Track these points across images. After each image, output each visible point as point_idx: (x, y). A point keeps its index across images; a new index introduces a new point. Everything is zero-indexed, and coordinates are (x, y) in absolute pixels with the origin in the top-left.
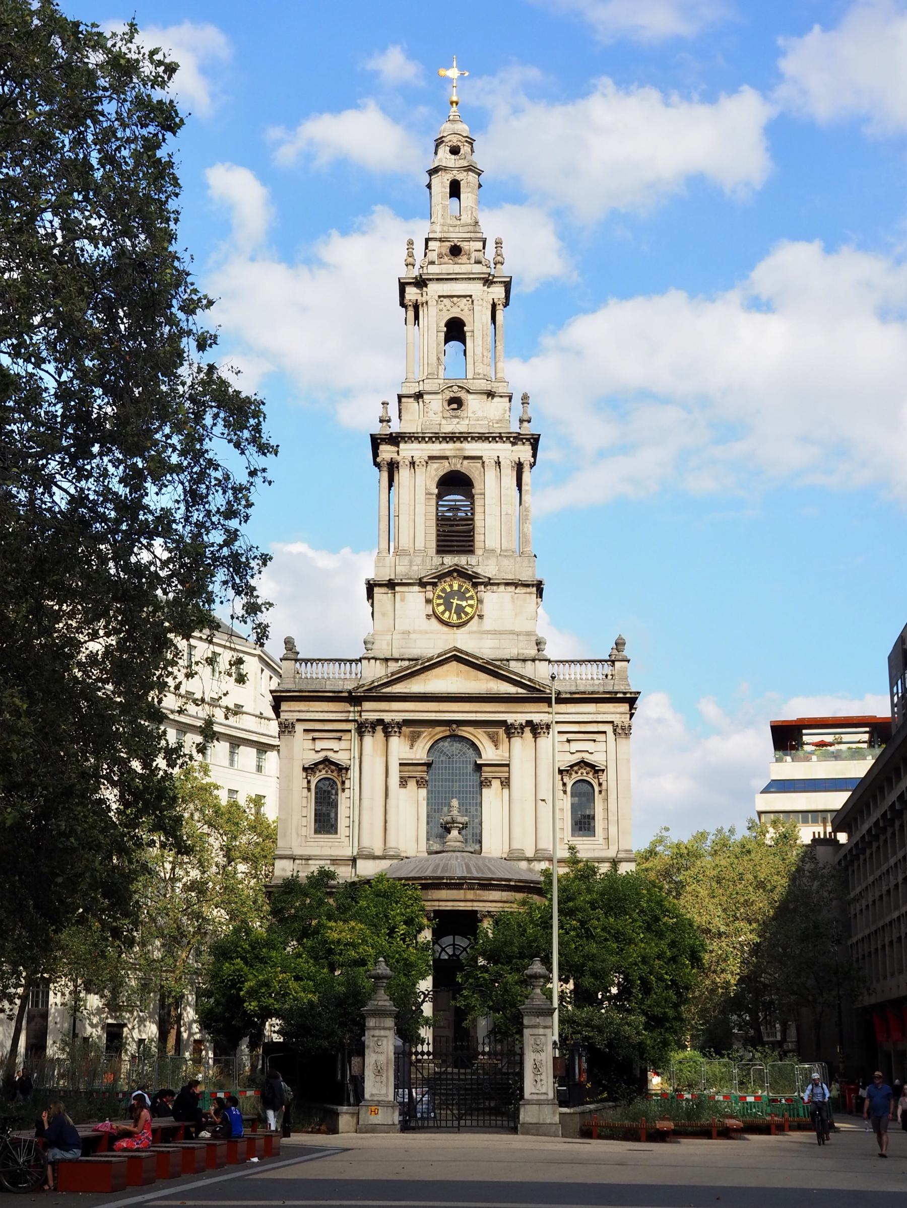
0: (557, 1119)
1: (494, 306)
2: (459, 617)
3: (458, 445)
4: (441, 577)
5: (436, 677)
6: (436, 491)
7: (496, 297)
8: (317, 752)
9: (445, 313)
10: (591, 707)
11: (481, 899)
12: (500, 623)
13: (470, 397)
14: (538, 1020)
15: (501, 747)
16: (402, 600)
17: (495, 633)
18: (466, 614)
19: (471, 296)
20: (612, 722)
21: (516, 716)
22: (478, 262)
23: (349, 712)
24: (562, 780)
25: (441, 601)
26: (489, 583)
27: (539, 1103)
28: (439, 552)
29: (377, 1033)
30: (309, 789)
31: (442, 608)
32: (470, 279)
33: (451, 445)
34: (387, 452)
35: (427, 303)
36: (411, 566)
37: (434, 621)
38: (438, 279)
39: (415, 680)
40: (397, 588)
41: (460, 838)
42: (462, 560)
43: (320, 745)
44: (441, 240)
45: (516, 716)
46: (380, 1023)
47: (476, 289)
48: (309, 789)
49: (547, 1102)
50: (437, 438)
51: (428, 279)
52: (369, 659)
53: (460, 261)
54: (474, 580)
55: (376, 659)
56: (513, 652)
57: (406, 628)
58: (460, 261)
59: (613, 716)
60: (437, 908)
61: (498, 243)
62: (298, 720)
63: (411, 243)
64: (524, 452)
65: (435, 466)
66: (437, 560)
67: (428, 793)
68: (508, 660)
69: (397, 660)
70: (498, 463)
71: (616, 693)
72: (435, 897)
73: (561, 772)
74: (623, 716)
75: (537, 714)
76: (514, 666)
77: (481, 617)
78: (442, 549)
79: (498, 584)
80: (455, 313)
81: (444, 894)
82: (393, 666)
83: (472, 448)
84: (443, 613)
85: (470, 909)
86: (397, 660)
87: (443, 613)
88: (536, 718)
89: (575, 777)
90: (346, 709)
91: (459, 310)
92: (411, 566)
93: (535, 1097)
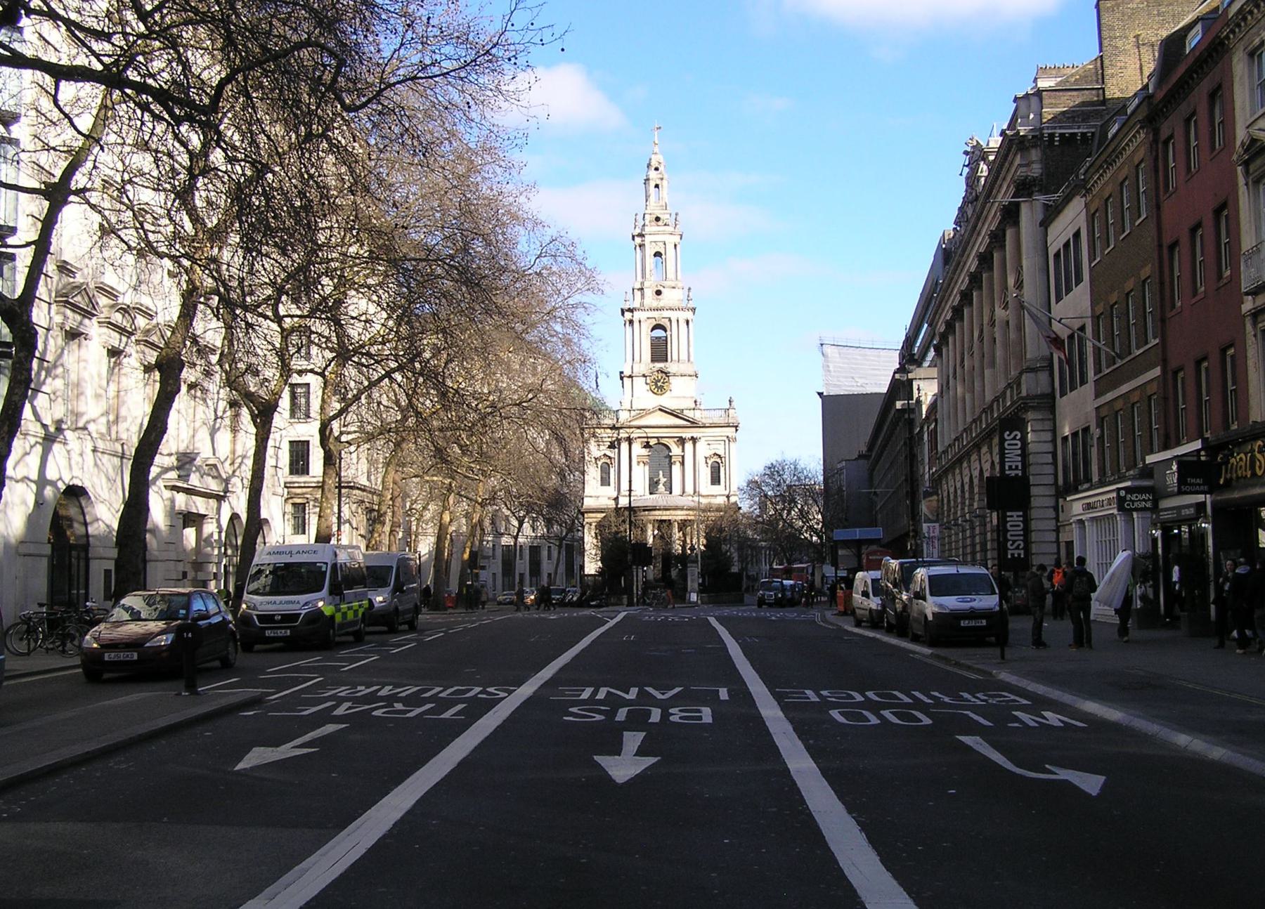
12: (679, 394)
28: (653, 361)
64: (689, 315)
66: (651, 365)
81: (657, 513)
82: (633, 413)
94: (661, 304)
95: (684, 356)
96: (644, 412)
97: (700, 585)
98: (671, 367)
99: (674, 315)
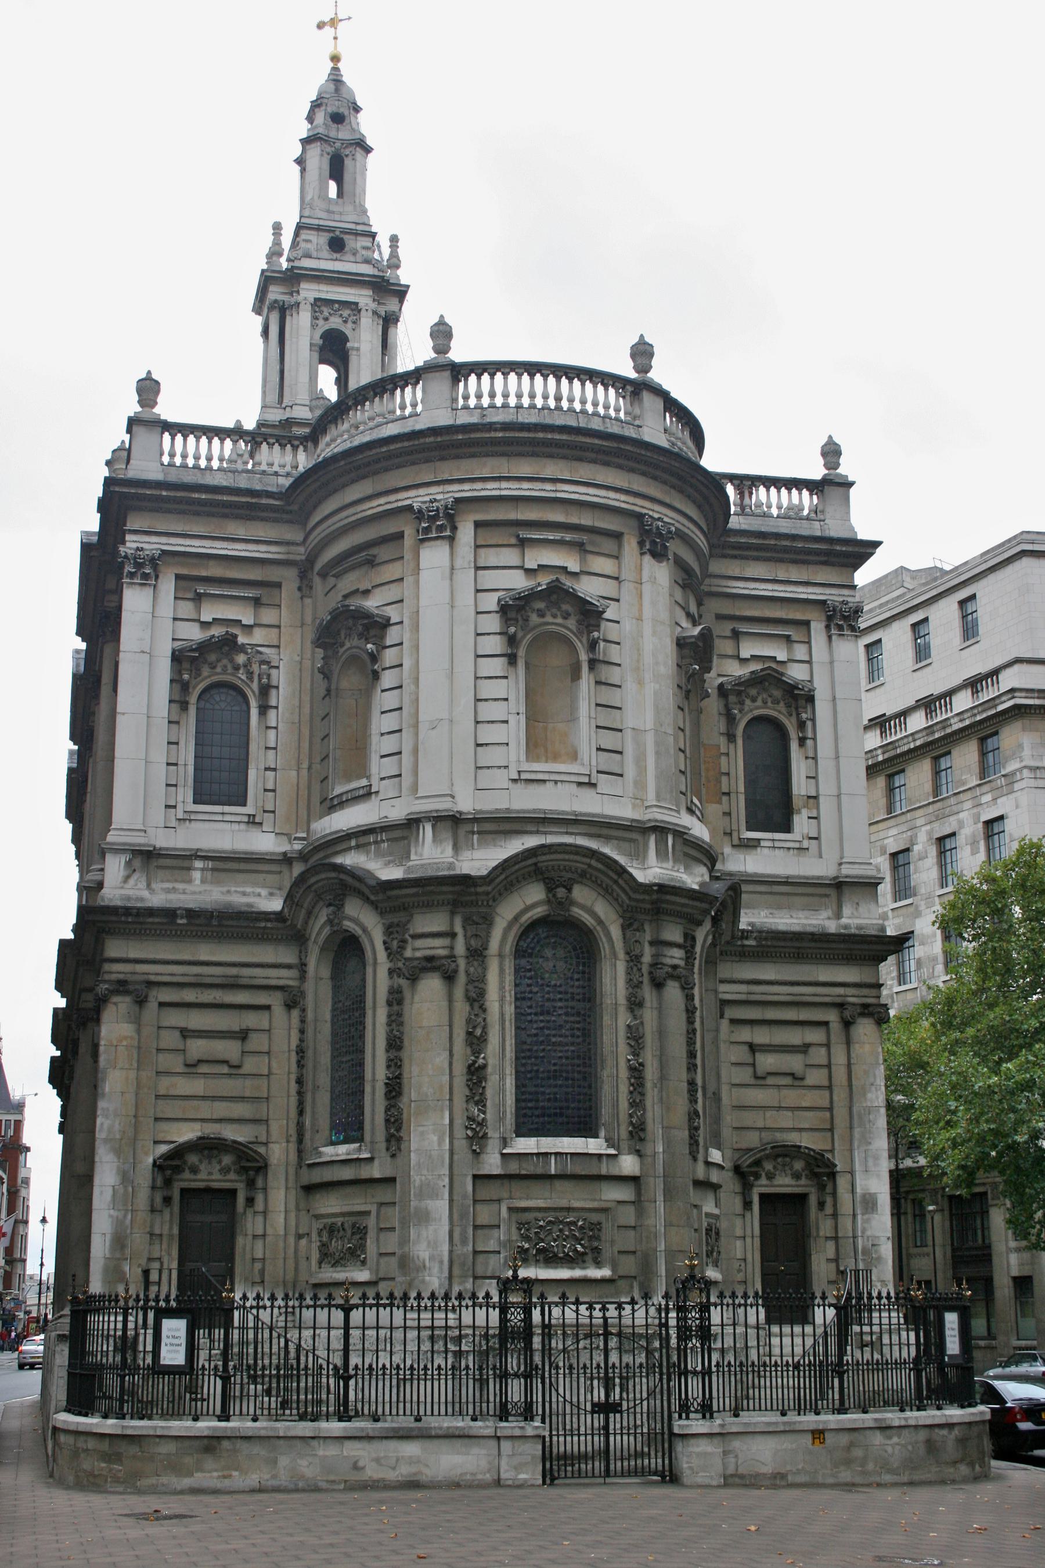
9: (321, 322)
19: (357, 304)
22: (367, 261)
35: (298, 304)
47: (363, 297)
61: (394, 240)
63: (277, 228)
80: (335, 322)
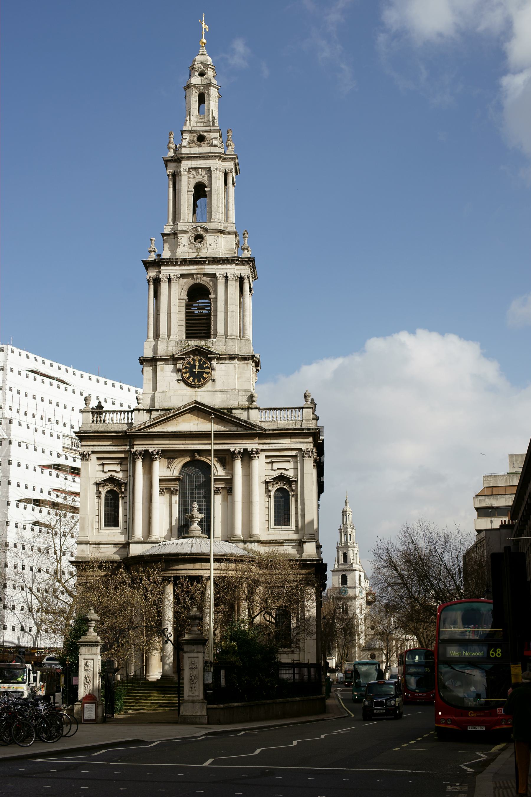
0: (204, 713)
1: (226, 174)
2: (199, 381)
3: (201, 267)
4: (187, 354)
5: (184, 421)
6: (186, 297)
7: (227, 168)
8: (106, 472)
10: (288, 441)
11: (205, 568)
13: (208, 235)
14: (193, 648)
15: (227, 467)
16: (162, 370)
17: (222, 391)
18: (204, 378)
20: (300, 450)
21: (236, 446)
23: (126, 445)
24: (267, 488)
25: (187, 370)
26: (220, 358)
27: (193, 702)
29: (87, 657)
30: (100, 498)
31: (188, 375)
32: (209, 156)
33: (195, 267)
34: (152, 273)
36: (167, 347)
37: (182, 383)
38: (188, 157)
39: (169, 423)
40: (158, 363)
41: (199, 528)
42: (201, 343)
43: (107, 468)
44: (190, 132)
45: (236, 446)
46: (89, 650)
48: (100, 498)
49: (198, 701)
50: (185, 262)
51: (181, 157)
52: (139, 410)
53: (203, 145)
54: (206, 355)
55: (144, 410)
56: (235, 404)
57: (164, 389)
58: (203, 145)
59: (302, 445)
60: (176, 575)
62: (93, 452)
64: (245, 271)
65: (185, 280)
67: (179, 498)
68: (232, 409)
69: (157, 410)
70: (226, 278)
71: (303, 429)
72: (174, 568)
73: (267, 483)
74: (308, 445)
75: (251, 445)
76: (235, 412)
77: (213, 380)
78: (189, 335)
79: (225, 359)
80: (199, 178)
82: (155, 414)
83: (209, 269)
84: (189, 378)
85: (197, 575)
86: (157, 410)
87: (189, 378)
88: (249, 447)
89: (277, 486)
90: (125, 444)
91: (201, 177)
92: (167, 347)
93: (191, 698)
94: (203, 254)
95: (234, 330)
96: (171, 414)
97: (206, 687)
98: (217, 345)
99: (219, 270)
